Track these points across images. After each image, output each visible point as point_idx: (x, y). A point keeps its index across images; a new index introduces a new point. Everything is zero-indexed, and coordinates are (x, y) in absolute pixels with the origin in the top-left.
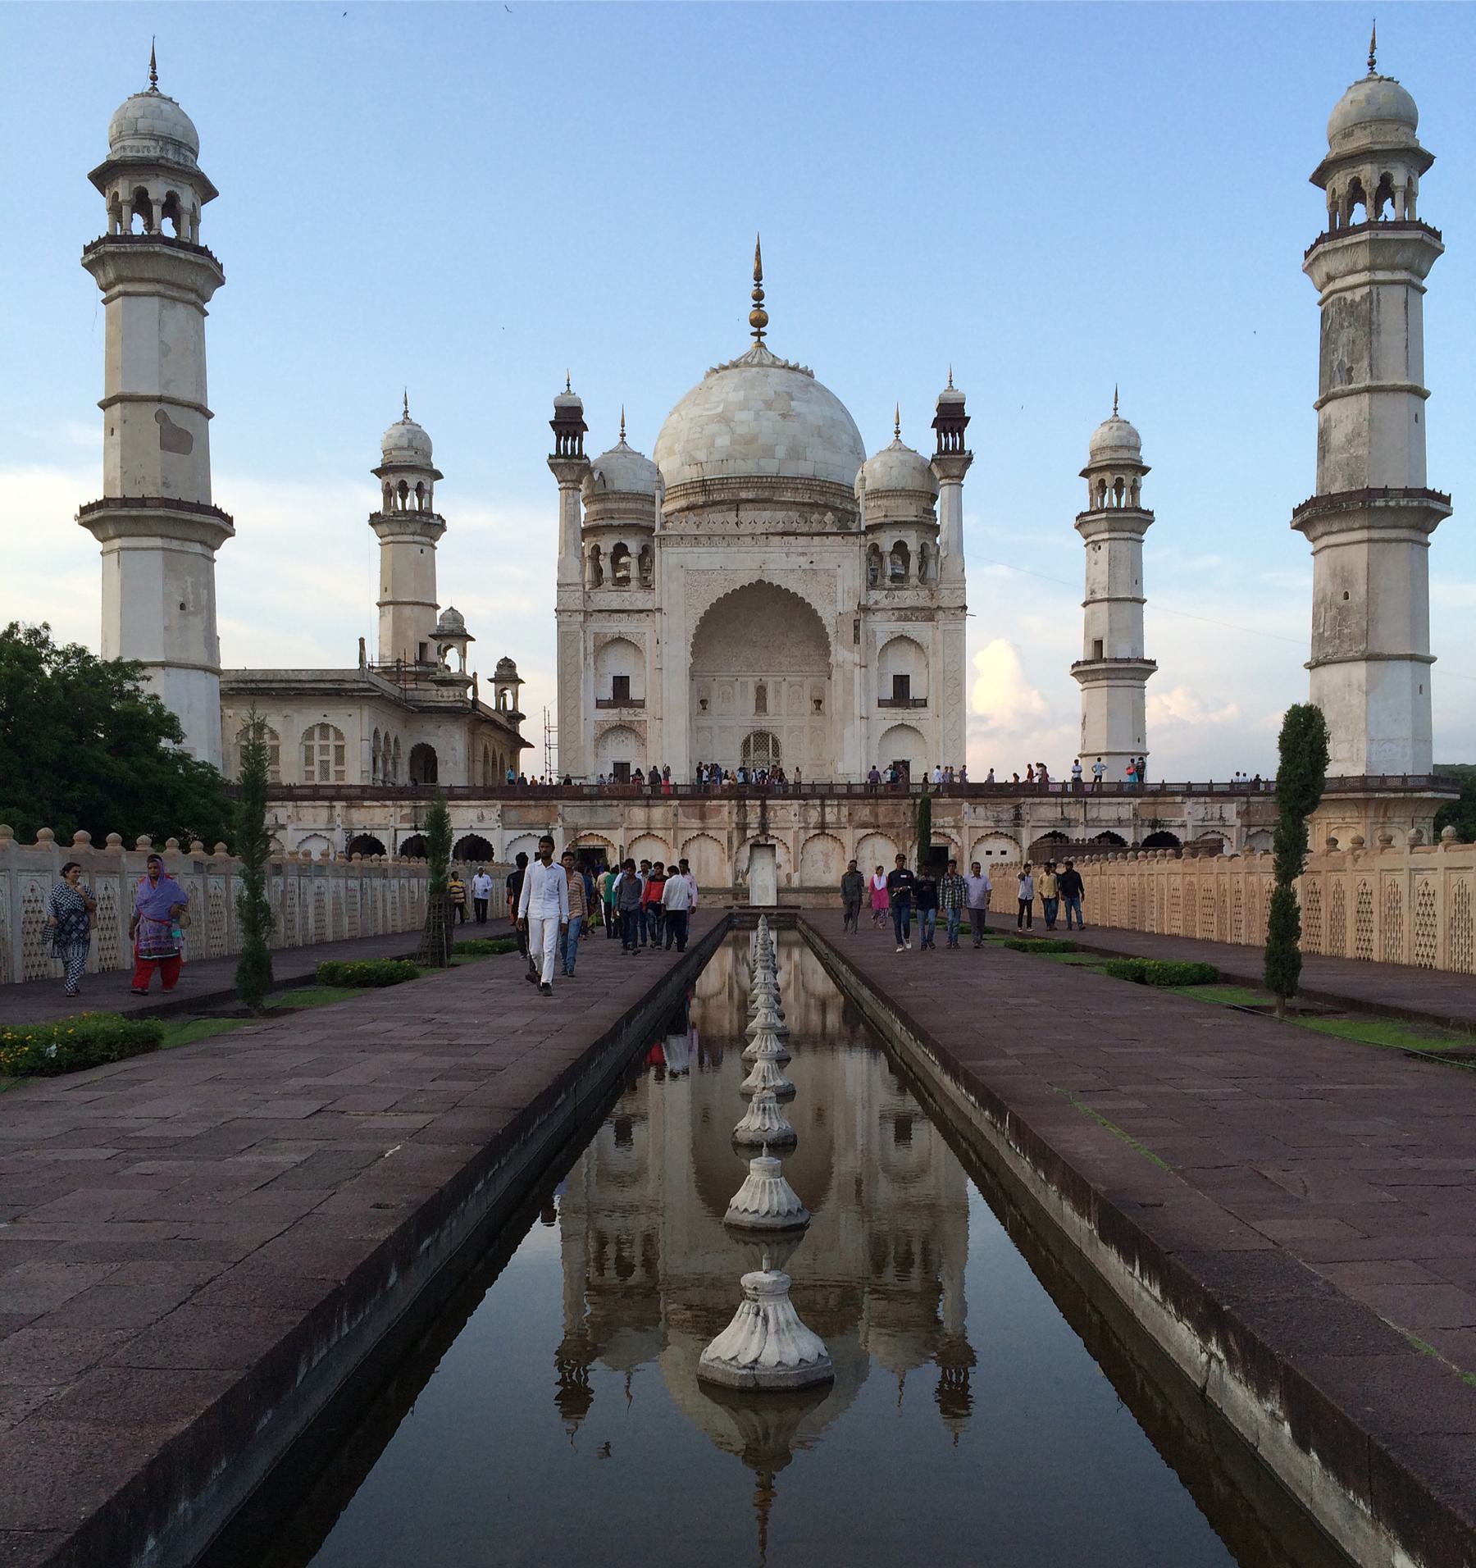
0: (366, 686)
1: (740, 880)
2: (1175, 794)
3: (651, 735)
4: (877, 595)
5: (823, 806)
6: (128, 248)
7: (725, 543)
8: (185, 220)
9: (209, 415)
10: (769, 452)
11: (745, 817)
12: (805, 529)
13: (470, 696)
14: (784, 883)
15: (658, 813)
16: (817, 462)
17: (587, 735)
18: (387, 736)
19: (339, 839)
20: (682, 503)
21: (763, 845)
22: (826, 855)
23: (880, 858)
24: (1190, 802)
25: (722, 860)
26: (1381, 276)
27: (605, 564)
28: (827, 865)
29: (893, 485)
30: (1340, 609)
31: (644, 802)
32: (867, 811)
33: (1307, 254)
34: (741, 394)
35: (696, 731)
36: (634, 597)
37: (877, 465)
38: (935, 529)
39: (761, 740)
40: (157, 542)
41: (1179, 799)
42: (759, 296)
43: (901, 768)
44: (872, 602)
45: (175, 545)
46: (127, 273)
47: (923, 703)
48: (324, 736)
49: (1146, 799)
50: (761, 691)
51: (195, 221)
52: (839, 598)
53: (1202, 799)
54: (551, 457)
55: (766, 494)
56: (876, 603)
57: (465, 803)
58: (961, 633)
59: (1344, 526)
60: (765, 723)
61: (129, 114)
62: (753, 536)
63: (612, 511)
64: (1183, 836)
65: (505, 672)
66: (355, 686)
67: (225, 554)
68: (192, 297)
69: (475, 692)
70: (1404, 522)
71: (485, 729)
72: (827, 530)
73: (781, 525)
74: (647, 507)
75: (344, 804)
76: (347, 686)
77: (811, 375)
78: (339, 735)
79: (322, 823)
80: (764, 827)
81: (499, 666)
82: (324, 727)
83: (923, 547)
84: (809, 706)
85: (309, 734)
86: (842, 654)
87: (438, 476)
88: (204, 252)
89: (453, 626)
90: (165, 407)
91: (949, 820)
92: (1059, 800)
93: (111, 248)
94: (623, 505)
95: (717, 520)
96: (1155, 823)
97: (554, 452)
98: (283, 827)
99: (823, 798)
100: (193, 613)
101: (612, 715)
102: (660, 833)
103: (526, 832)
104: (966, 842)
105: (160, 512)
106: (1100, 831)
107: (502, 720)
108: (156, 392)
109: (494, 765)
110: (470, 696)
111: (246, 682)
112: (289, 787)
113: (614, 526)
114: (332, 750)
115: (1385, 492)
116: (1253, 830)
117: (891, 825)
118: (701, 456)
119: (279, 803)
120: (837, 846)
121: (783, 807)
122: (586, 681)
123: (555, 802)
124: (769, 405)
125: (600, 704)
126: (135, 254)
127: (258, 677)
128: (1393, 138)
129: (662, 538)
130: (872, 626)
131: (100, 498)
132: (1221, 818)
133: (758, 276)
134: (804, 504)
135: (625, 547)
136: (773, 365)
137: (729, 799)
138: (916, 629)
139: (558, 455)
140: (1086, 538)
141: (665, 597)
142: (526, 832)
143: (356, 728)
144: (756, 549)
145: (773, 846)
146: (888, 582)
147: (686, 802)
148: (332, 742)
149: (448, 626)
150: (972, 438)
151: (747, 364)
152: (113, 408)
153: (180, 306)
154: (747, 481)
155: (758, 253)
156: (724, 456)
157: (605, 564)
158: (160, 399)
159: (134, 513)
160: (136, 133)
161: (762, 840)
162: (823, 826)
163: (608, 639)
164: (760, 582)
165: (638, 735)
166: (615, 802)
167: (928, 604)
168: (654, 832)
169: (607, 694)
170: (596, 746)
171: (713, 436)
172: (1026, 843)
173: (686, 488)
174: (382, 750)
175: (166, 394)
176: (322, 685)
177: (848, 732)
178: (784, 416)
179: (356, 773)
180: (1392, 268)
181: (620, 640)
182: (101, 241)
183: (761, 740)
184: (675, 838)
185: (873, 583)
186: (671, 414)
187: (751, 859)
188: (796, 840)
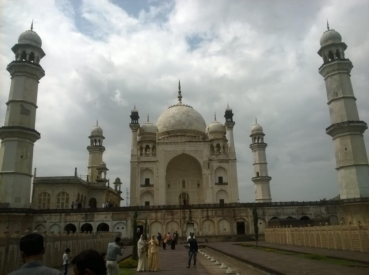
0: (76, 181)
3: (155, 194)
4: (214, 157)
7: (174, 144)
9: (37, 107)
10: (184, 124)
11: (185, 215)
12: (195, 141)
15: (159, 214)
16: (195, 127)
17: (138, 194)
18: (82, 195)
19: (63, 225)
21: (190, 223)
22: (209, 226)
23: (226, 227)
26: (341, 71)
28: (209, 229)
31: (155, 211)
33: (319, 69)
35: (168, 193)
40: (16, 139)
41: (309, 206)
43: (222, 201)
44: (212, 158)
45: (21, 140)
46: (17, 70)
47: (227, 184)
48: (63, 195)
49: (299, 207)
50: (184, 183)
53: (315, 206)
55: (184, 134)
56: (213, 158)
58: (235, 166)
60: (185, 190)
62: (181, 142)
63: (146, 137)
64: (312, 217)
66: (73, 181)
71: (111, 194)
73: (188, 140)
75: (65, 214)
78: (67, 195)
79: (57, 220)
80: (190, 218)
82: (63, 193)
83: (224, 145)
84: (196, 186)
85: (59, 195)
86: (205, 171)
87: (104, 138)
91: (244, 214)
92: (275, 207)
94: (148, 136)
95: (173, 139)
97: (131, 123)
98: (46, 222)
99: (207, 208)
101: (145, 189)
102: (160, 221)
103: (119, 221)
104: (250, 220)
106: (288, 216)
107: (116, 193)
110: (107, 185)
111: (42, 181)
113: (146, 141)
114: (65, 199)
116: (330, 215)
118: (167, 125)
119: (45, 214)
121: (196, 211)
123: (128, 212)
124: (184, 113)
125: (142, 186)
127: (46, 179)
129: (158, 143)
132: (321, 212)
134: (193, 136)
135: (149, 146)
137: (180, 209)
138: (223, 165)
139: (132, 123)
140: (252, 150)
142: (119, 221)
144: (182, 146)
145: (193, 223)
147: (167, 211)
148: (65, 197)
150: (234, 119)
151: (177, 105)
154: (179, 131)
158: (22, 101)
162: (208, 217)
163: (144, 168)
164: (184, 154)
166: (146, 211)
167: (226, 158)
168: (158, 220)
169: (144, 183)
170: (140, 197)
172: (267, 220)
173: (164, 133)
175: (24, 100)
176: (64, 181)
178: (187, 116)
181: (147, 169)
188: (200, 221)
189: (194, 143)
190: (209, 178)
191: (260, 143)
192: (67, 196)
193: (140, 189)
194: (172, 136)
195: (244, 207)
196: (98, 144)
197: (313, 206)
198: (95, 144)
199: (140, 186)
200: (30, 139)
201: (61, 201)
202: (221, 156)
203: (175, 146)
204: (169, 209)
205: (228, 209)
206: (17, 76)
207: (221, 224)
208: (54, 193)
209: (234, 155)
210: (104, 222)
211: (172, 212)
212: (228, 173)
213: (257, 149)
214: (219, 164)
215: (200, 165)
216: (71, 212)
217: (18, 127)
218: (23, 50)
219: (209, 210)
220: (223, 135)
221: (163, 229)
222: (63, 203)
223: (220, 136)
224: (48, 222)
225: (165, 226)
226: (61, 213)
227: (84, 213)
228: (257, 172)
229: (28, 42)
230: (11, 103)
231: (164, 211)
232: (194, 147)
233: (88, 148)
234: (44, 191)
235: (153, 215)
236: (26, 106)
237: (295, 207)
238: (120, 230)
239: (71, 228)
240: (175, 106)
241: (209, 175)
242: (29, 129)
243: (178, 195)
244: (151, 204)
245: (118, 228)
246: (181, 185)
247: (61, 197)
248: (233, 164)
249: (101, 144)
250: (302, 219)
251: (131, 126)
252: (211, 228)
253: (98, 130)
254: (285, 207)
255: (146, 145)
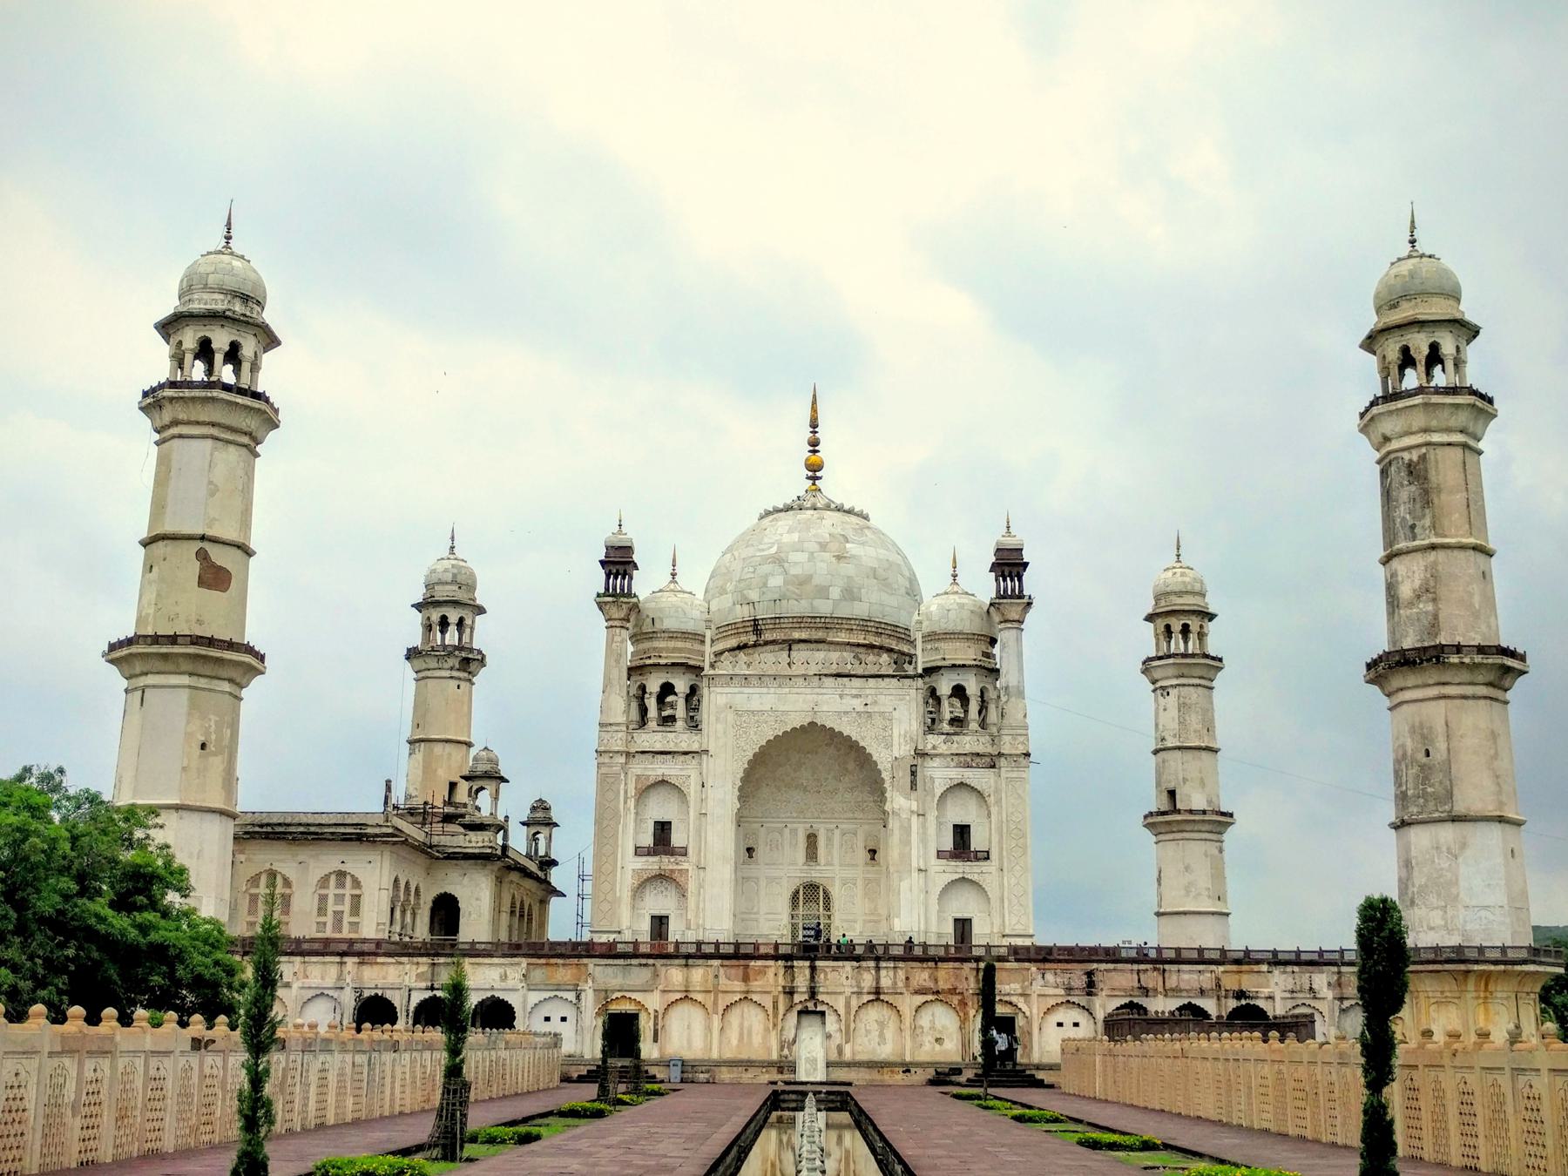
0: (390, 831)
1: (786, 1052)
2: (1258, 962)
3: (692, 887)
4: (933, 740)
5: (878, 968)
6: (187, 393)
8: (246, 367)
10: (823, 592)
12: (860, 672)
13: (500, 842)
14: (834, 1057)
16: (874, 603)
17: (625, 882)
19: (349, 1000)
20: (733, 642)
21: (812, 1011)
22: (882, 1025)
24: (1277, 971)
25: (767, 1030)
26: (1436, 438)
27: (651, 703)
28: (882, 1035)
29: (951, 627)
30: (1422, 767)
31: (683, 962)
32: (925, 975)
33: (1362, 415)
34: (795, 537)
35: (742, 882)
36: (679, 738)
37: (933, 608)
38: (994, 672)
39: (811, 892)
40: (185, 680)
41: (1264, 968)
42: (814, 443)
43: (963, 927)
44: (929, 746)
45: (202, 683)
46: (182, 416)
48: (341, 885)
50: (812, 839)
51: (255, 368)
52: (895, 742)
53: (1289, 969)
54: (599, 595)
55: (820, 635)
57: (487, 960)
59: (1420, 682)
60: (816, 874)
61: (201, 270)
62: (805, 677)
65: (540, 815)
66: (377, 831)
67: (255, 693)
68: (245, 440)
69: (505, 837)
70: (1480, 679)
71: (514, 876)
72: (883, 672)
74: (697, 646)
75: (356, 959)
76: (369, 830)
77: (866, 518)
78: (357, 883)
79: (330, 981)
80: (813, 993)
81: (534, 809)
82: (341, 875)
84: (863, 855)
86: (898, 801)
88: (257, 396)
89: (487, 767)
90: (207, 546)
91: (1015, 987)
92: (1135, 967)
93: (169, 393)
94: (672, 644)
95: (769, 660)
96: (1240, 994)
99: (878, 959)
100: (215, 754)
101: (653, 864)
102: (699, 997)
104: (1035, 1011)
105: (192, 650)
108: (199, 530)
109: (522, 916)
111: (261, 826)
112: (298, 941)
114: (348, 900)
115: (1458, 649)
117: (953, 991)
118: (753, 595)
120: (894, 1017)
121: (834, 969)
122: (625, 826)
123: (585, 961)
124: (823, 547)
125: (639, 852)
126: (193, 399)
127: (275, 820)
128: (1436, 309)
130: (928, 773)
131: (131, 634)
133: (814, 425)
134: (859, 645)
136: (828, 507)
138: (979, 777)
141: (712, 740)
143: (375, 874)
145: (823, 1014)
146: (946, 727)
147: (726, 962)
148: (348, 891)
149: (482, 768)
150: (1031, 581)
152: (154, 546)
153: (232, 448)
154: (800, 621)
155: (814, 402)
156: (776, 596)
157: (651, 703)
158: (203, 538)
159: (164, 650)
160: (206, 287)
161: (811, 1006)
162: (877, 992)
163: (651, 781)
164: (812, 724)
165: (678, 885)
166: (651, 961)
167: (989, 750)
168: (691, 995)
169: (648, 840)
170: (634, 897)
171: (766, 577)
172: (1100, 1015)
174: (401, 901)
175: (210, 533)
176: (342, 830)
177: (904, 885)
178: (839, 558)
179: (372, 924)
180: (1449, 430)
181: (663, 782)
182: (161, 386)
183: (811, 892)
184: (715, 1003)
185: (931, 727)
186: (724, 554)
187: (798, 1027)
189: (856, 682)
190: (916, 831)
191: (1193, 656)
192: (353, 888)
193: (631, 866)
194: (773, 642)
195: (1017, 960)
196: (452, 637)
197: (1282, 968)
198: (443, 639)
199: (631, 850)
200: (231, 681)
201: (331, 907)
202: (967, 738)
203: (779, 691)
204: (739, 955)
205: (957, 965)
206: (181, 436)
207: (925, 1019)
208: (304, 872)
209: (1021, 739)
210: (497, 994)
211: (747, 966)
212: (994, 810)
213: (1175, 682)
214: (957, 774)
215: (879, 772)
216: (376, 954)
217: (196, 640)
218: (201, 334)
219: (883, 964)
220: (984, 647)
221: (709, 1029)
222: (338, 916)
223: (968, 653)
224: (295, 986)
225: (716, 1019)
226: (343, 954)
227: (424, 959)
228: (1171, 786)
229: (219, 303)
230: (161, 543)
231: (716, 962)
232: (856, 696)
233: (412, 654)
234: (268, 866)
235: (675, 974)
236: (219, 556)
237: (1213, 967)
238: (556, 1026)
239: (374, 1010)
240: (788, 509)
241: (914, 818)
242: (231, 646)
243: (787, 895)
244: (675, 932)
245: (547, 1019)
246: (801, 854)
247: (332, 891)
248: (1014, 775)
249: (466, 638)
250: (1235, 1014)
251: (601, 606)
252: (889, 1033)
253: (455, 575)
254: (1174, 967)
255: (661, 681)
